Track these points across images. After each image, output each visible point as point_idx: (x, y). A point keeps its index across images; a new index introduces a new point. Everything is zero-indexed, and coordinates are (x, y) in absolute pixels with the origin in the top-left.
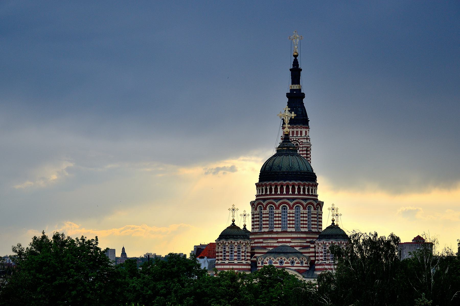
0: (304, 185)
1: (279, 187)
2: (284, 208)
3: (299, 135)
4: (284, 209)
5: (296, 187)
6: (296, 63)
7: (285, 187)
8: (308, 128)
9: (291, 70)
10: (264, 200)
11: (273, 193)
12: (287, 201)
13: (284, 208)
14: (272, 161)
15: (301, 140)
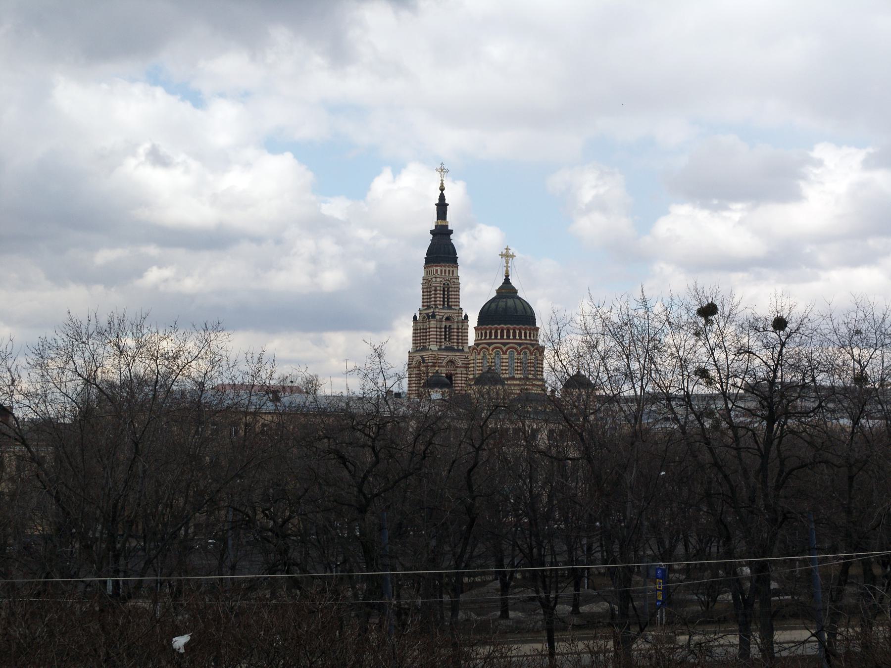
0: (525, 329)
1: (499, 331)
2: (525, 353)
3: (451, 275)
4: (525, 354)
5: (517, 332)
6: (442, 197)
7: (505, 331)
8: (457, 267)
9: (436, 204)
10: (505, 344)
11: (493, 337)
12: (516, 346)
13: (525, 353)
14: (489, 304)
15: (454, 280)
